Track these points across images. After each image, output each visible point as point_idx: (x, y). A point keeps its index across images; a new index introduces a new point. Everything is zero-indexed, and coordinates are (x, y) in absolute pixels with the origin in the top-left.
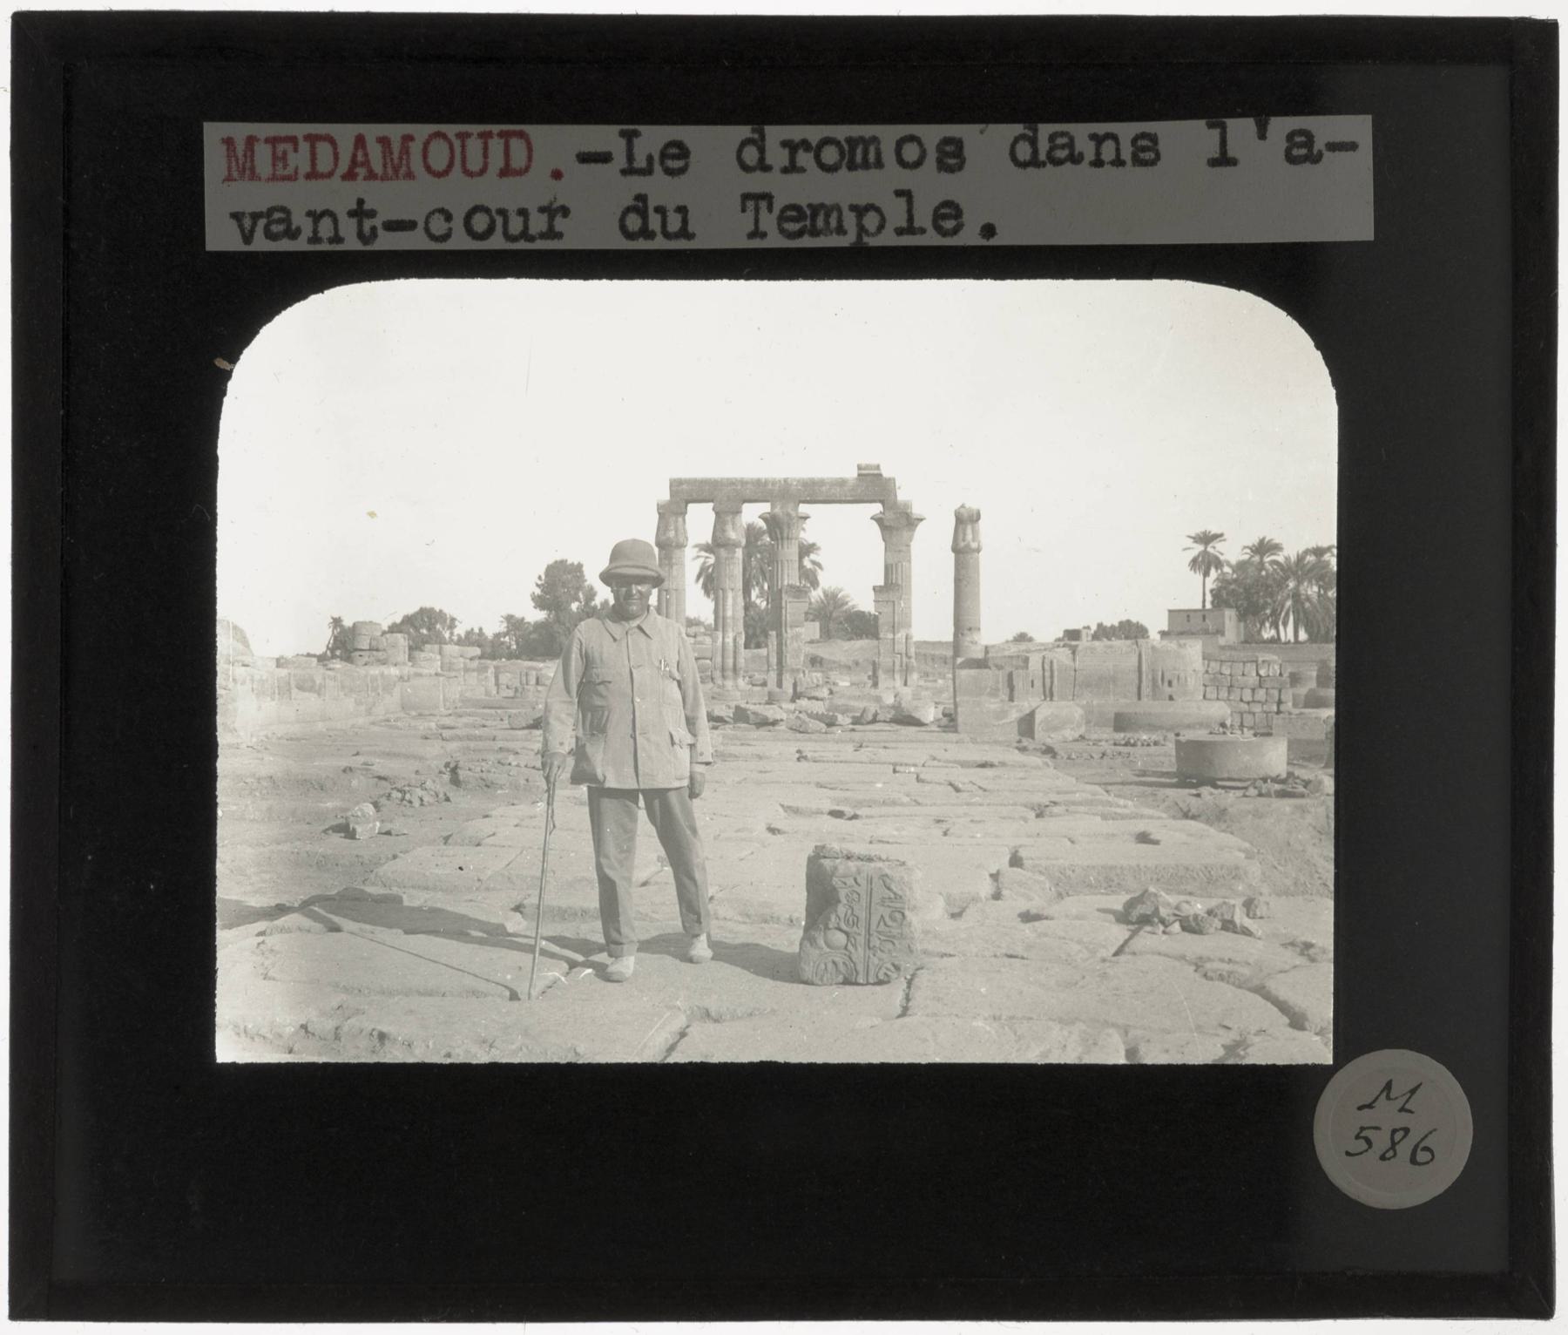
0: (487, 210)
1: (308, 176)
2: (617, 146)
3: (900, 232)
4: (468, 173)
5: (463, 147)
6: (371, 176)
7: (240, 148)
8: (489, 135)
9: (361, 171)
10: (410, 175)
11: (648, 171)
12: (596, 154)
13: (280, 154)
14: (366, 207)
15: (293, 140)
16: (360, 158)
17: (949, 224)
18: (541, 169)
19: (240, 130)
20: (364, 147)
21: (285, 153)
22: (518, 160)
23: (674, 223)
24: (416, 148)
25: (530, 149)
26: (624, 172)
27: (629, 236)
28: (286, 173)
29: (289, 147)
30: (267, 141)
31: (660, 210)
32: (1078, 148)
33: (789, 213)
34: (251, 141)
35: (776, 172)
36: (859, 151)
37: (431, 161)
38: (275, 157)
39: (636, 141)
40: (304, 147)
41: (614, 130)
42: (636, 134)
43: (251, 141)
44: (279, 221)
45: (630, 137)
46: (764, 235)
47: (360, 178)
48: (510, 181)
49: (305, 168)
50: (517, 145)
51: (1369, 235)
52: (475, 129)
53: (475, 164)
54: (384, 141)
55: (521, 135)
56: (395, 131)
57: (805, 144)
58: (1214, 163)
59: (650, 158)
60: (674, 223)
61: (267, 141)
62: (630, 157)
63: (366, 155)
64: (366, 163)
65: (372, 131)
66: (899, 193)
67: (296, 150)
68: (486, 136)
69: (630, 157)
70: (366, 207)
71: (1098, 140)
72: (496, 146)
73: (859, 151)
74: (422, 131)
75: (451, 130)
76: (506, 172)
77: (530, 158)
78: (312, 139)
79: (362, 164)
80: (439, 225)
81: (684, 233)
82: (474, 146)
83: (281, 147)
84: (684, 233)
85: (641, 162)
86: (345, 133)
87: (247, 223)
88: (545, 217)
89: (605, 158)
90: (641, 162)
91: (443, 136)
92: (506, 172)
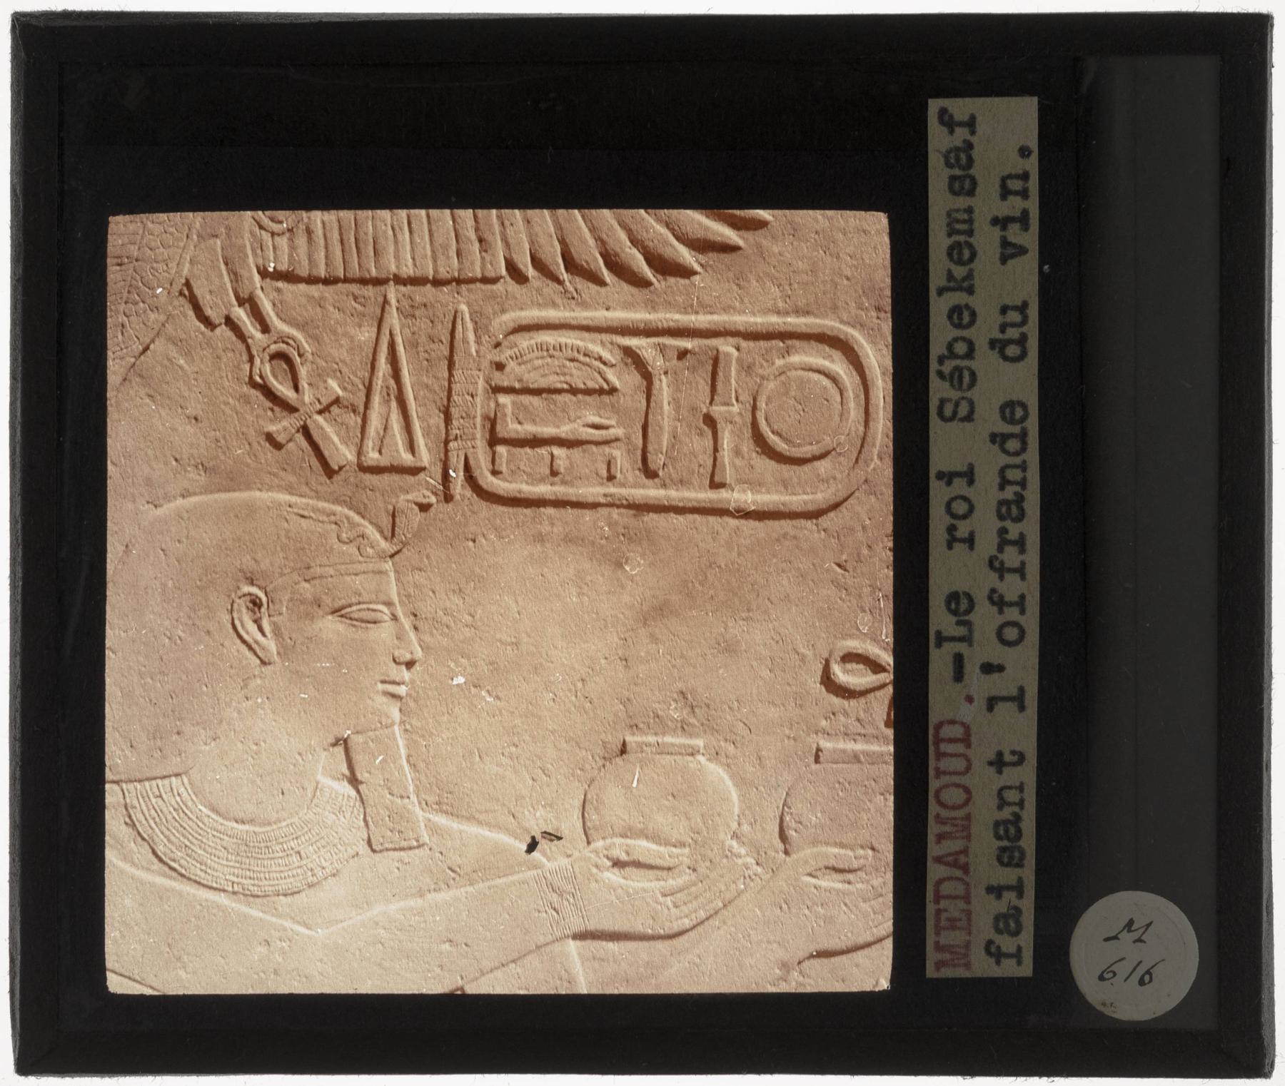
2: (950, 648)
5: (945, 773)
9: (962, 859)
11: (968, 624)
15: (939, 912)
16: (950, 859)
19: (932, 956)
21: (948, 919)
22: (957, 731)
23: (1014, 316)
24: (945, 813)
27: (1023, 356)
28: (964, 918)
29: (944, 916)
31: (1003, 328)
32: (959, 143)
34: (939, 947)
35: (974, 140)
36: (958, 226)
37: (959, 501)
38: (953, 928)
40: (943, 904)
41: (934, 653)
42: (938, 633)
45: (941, 639)
49: (962, 904)
52: (932, 763)
53: (959, 764)
54: (940, 837)
55: (939, 726)
56: (933, 829)
57: (951, 529)
58: (972, 547)
59: (959, 623)
60: (1014, 316)
62: (961, 639)
63: (950, 854)
65: (933, 849)
66: (990, 708)
67: (946, 910)
68: (940, 755)
69: (961, 639)
72: (944, 747)
73: (958, 226)
74: (933, 808)
75: (934, 784)
76: (966, 740)
81: (1023, 308)
82: (945, 764)
83: (943, 923)
84: (1023, 308)
85: (961, 631)
87: (1010, 251)
89: (959, 660)
90: (961, 631)
91: (938, 792)
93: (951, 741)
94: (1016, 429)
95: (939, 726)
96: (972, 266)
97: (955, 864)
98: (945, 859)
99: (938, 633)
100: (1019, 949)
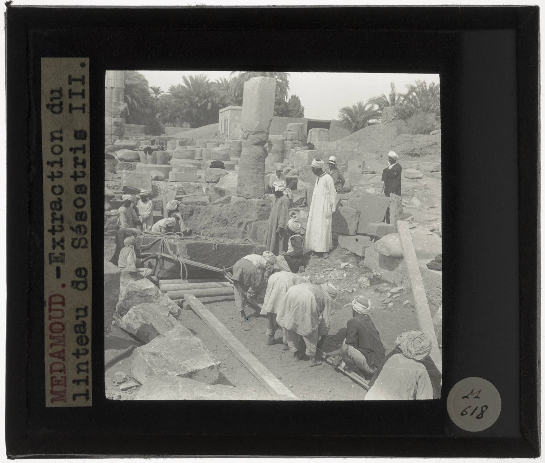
2: (55, 265)
16: (57, 355)
25: (56, 295)
29: (54, 379)
40: (55, 374)
50: (53, 300)
53: (59, 314)
54: (52, 345)
63: (57, 353)
64: (59, 353)
67: (55, 377)
72: (54, 307)
86: (48, 360)
89: (58, 269)
94: (83, 279)
97: (59, 357)
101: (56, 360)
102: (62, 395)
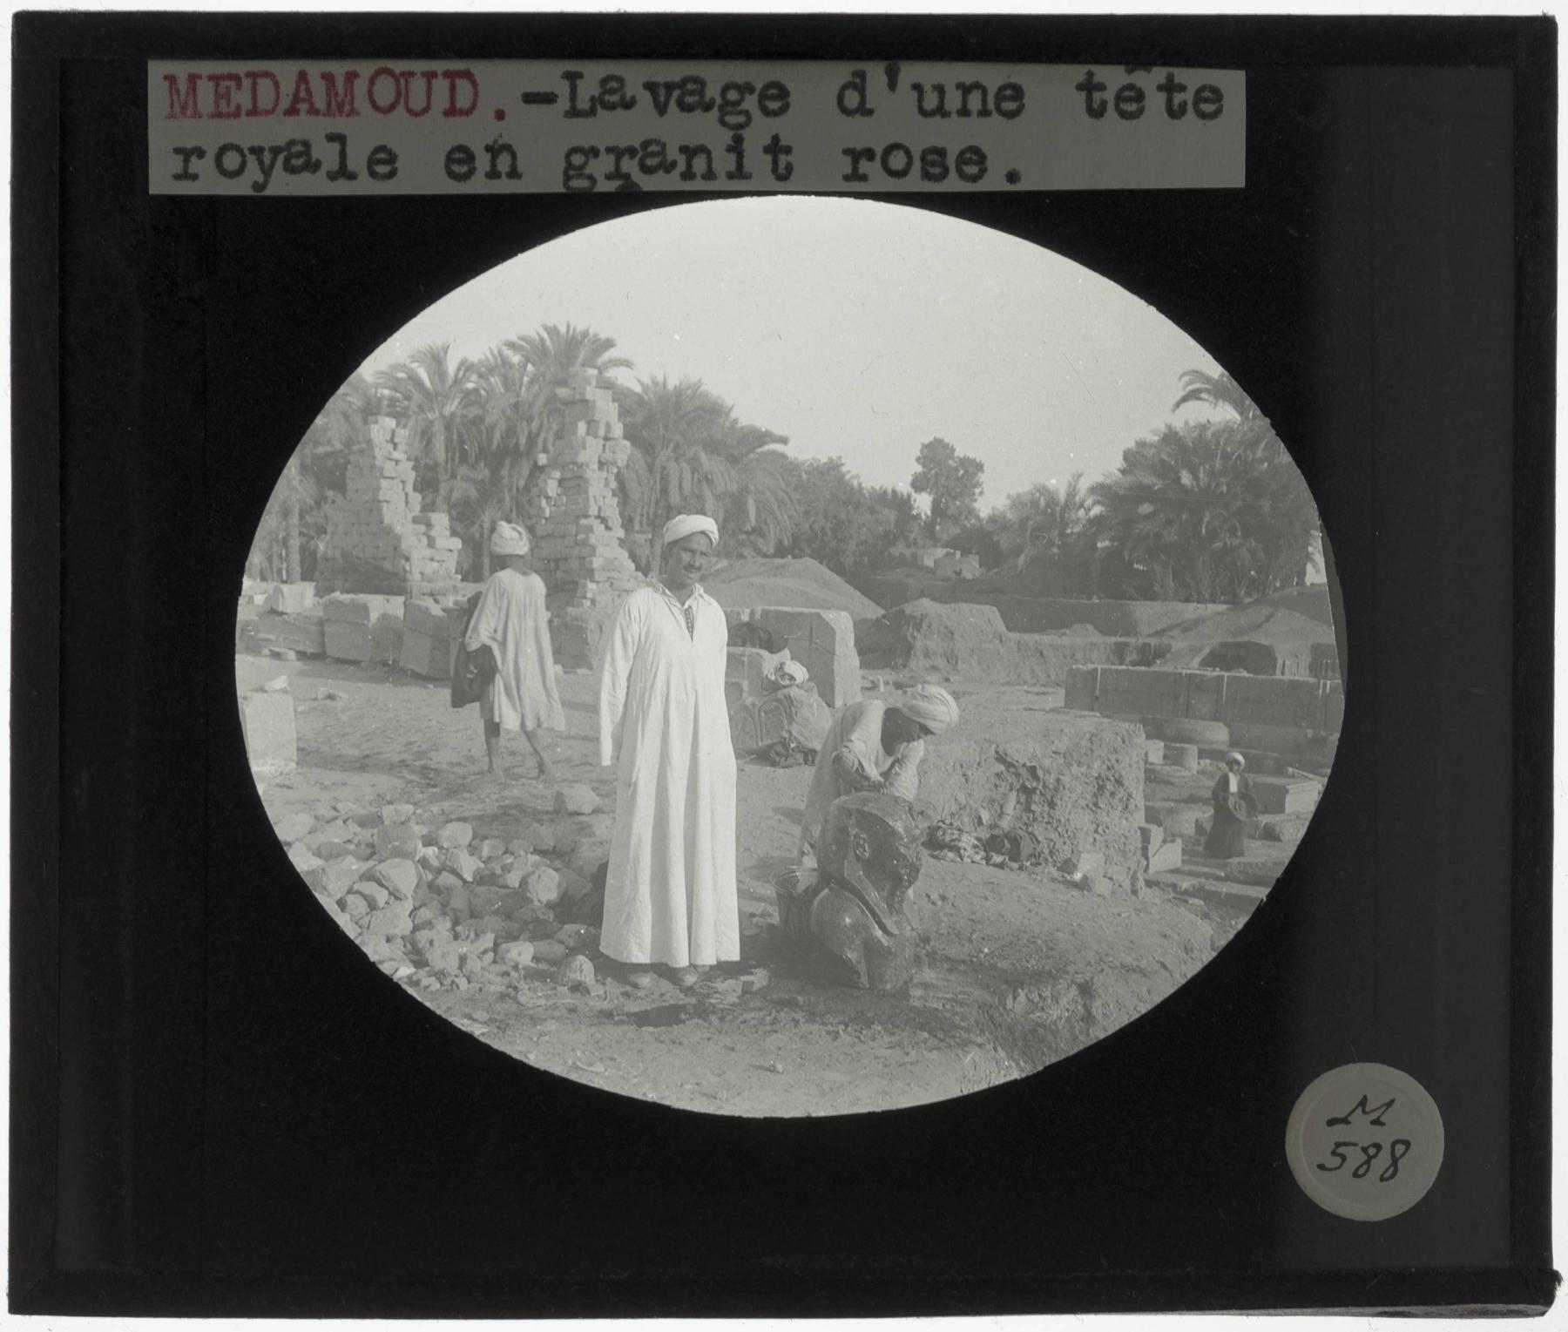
0: (238, 149)
1: (249, 114)
2: (562, 89)
3: (332, 177)
4: (409, 111)
6: (313, 111)
7: (183, 85)
8: (429, 76)
9: (303, 107)
10: (353, 112)
11: (592, 112)
12: (538, 94)
13: (222, 90)
14: (783, 143)
15: (237, 78)
16: (303, 94)
17: (972, 170)
18: (485, 110)
19: (181, 69)
20: (307, 82)
21: (228, 88)
22: (463, 101)
24: (360, 86)
26: (447, 113)
29: (233, 84)
30: (211, 78)
33: (457, 156)
34: (193, 79)
39: (579, 82)
40: (247, 83)
42: (580, 75)
43: (193, 79)
44: (299, 155)
45: (572, 77)
46: (352, 177)
47: (303, 113)
48: (458, 120)
49: (247, 104)
50: (463, 86)
51: (1238, 181)
54: (328, 78)
55: (467, 75)
56: (338, 68)
61: (211, 78)
63: (308, 90)
64: (310, 97)
65: (315, 68)
67: (239, 86)
68: (429, 76)
70: (783, 143)
71: (966, 90)
72: (441, 85)
74: (366, 68)
76: (451, 111)
77: (476, 94)
78: (253, 76)
79: (304, 100)
80: (897, 161)
82: (418, 86)
85: (583, 104)
88: (612, 158)
89: (548, 99)
90: (583, 104)
92: (451, 111)
93: (453, 89)
95: (467, 75)
96: (995, 114)
97: (296, 99)
98: (303, 87)
99: (580, 75)
100: (194, 177)
101: (288, 87)
102: (184, 107)
